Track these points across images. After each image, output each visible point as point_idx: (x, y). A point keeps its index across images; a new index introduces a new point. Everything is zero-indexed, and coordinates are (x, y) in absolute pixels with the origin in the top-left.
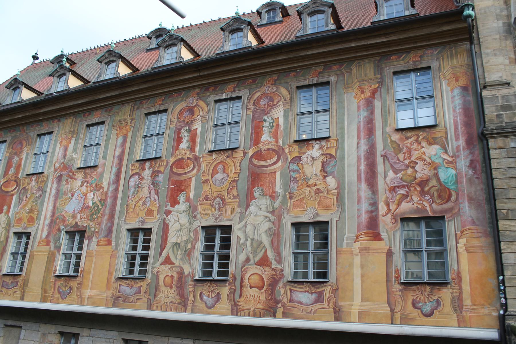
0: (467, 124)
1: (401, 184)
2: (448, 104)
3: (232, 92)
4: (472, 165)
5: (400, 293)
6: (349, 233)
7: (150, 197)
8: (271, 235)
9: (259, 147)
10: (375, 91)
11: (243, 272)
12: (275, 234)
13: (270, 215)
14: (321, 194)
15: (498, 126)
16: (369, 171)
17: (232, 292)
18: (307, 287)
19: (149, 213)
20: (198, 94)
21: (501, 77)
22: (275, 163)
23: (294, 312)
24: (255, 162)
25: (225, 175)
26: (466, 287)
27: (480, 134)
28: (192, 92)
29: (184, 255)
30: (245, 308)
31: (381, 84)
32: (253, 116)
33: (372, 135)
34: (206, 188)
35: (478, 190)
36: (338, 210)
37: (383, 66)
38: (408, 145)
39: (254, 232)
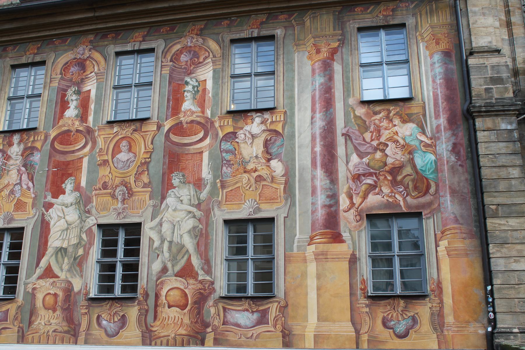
0: (449, 99)
1: (367, 171)
2: (426, 72)
3: (141, 42)
4: (455, 149)
6: (301, 234)
7: (20, 184)
8: (196, 236)
9: (179, 118)
10: (334, 52)
11: (159, 286)
12: (201, 235)
13: (194, 210)
14: (264, 183)
15: (487, 103)
16: (326, 153)
17: (143, 314)
18: (246, 304)
19: (20, 206)
20: (91, 42)
21: (490, 42)
22: (201, 140)
23: (229, 338)
24: (174, 138)
25: (131, 155)
26: (448, 300)
27: (465, 112)
28: (83, 39)
29: (73, 264)
30: (162, 334)
31: (342, 42)
32: (170, 76)
33: (331, 108)
34: (104, 172)
35: (462, 180)
36: (286, 203)
38: (377, 121)
39: (174, 233)
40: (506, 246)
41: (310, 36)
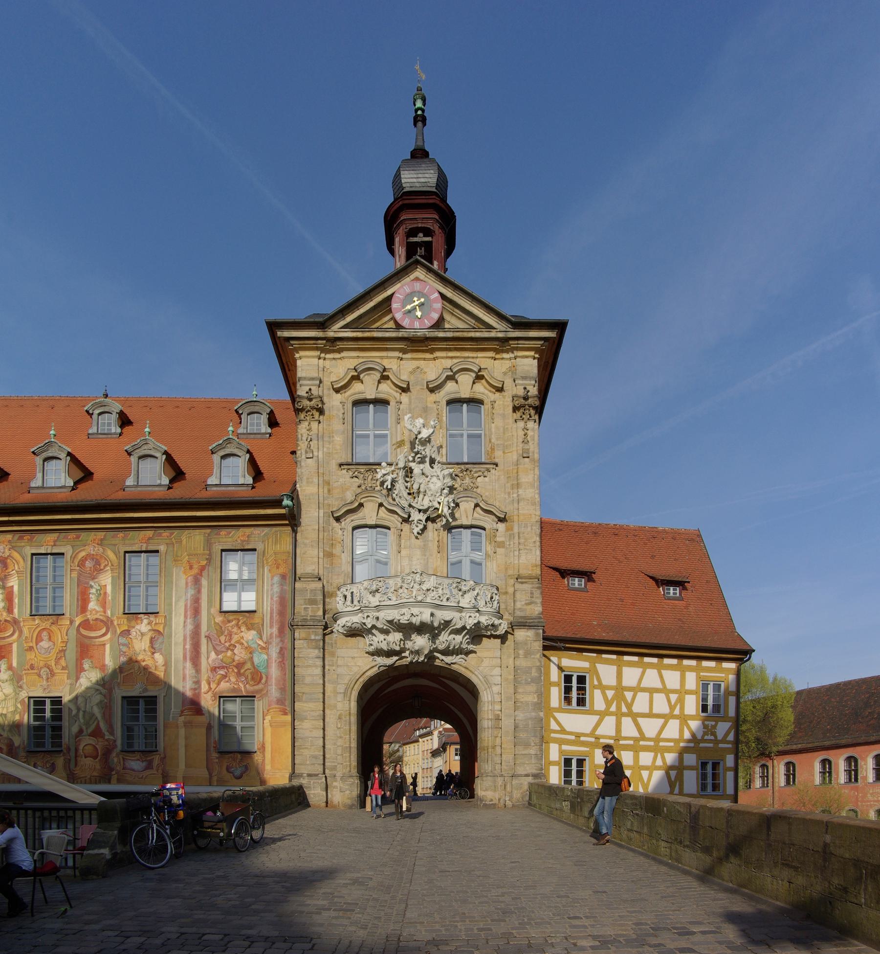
0: (282, 613)
2: (267, 591)
10: (202, 569)
18: (138, 755)
31: (209, 560)
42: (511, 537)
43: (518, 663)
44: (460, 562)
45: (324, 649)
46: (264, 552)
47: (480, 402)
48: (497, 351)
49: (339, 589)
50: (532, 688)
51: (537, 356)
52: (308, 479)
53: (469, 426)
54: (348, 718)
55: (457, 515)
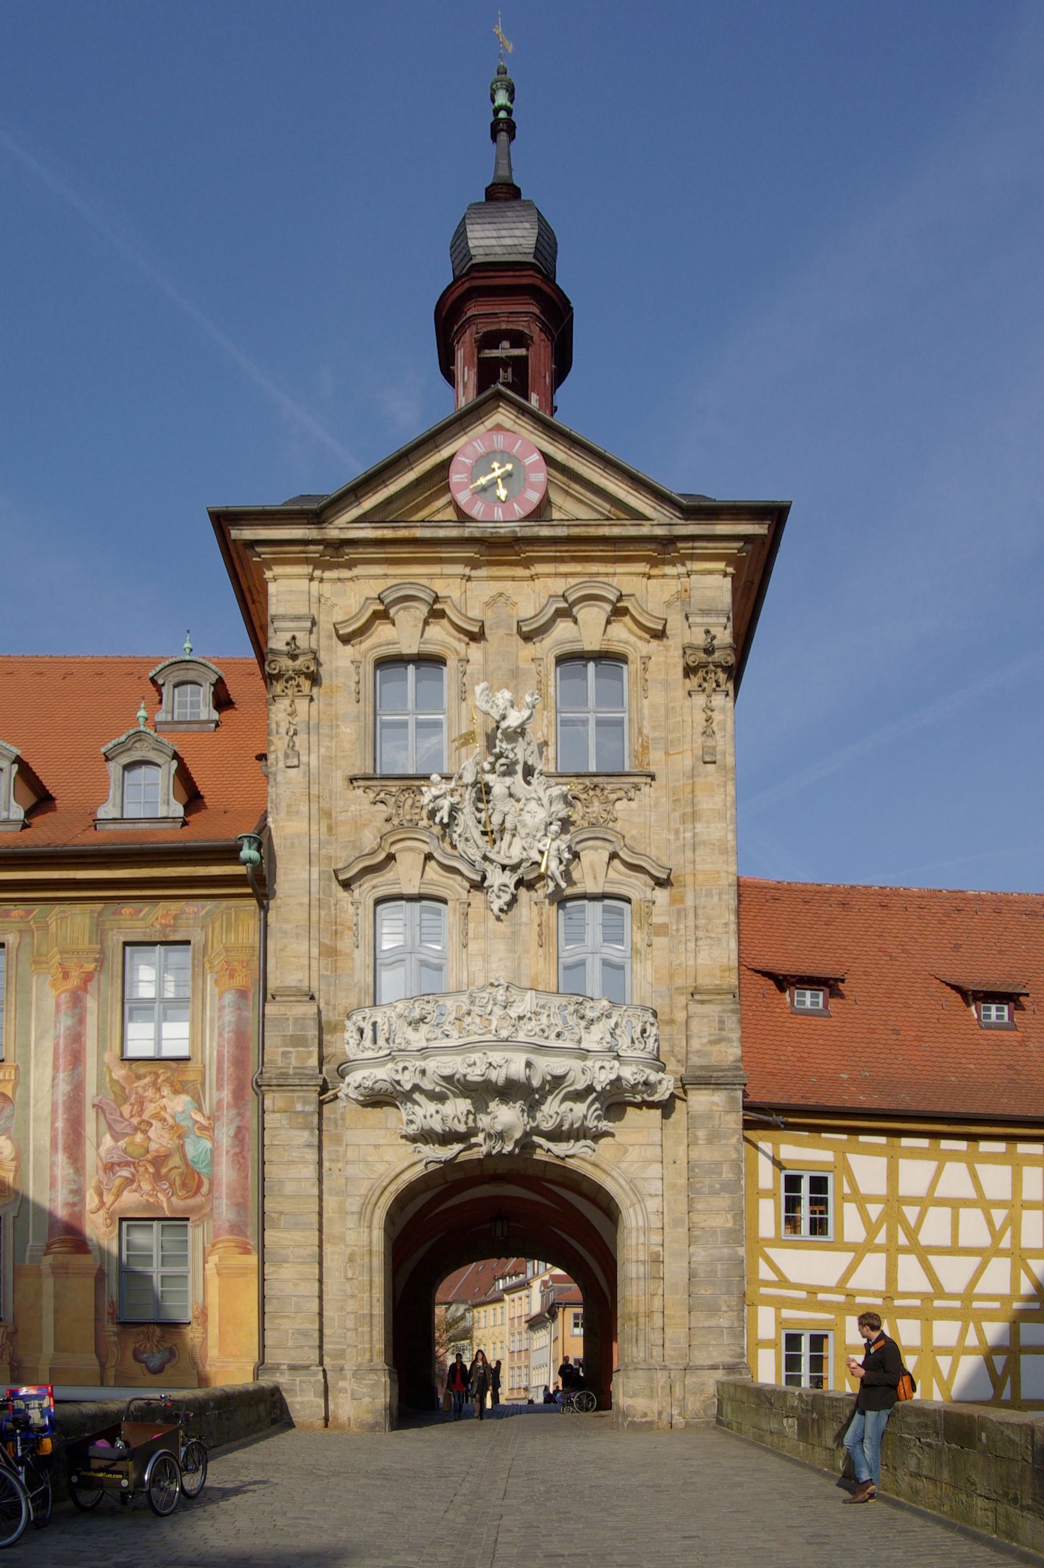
0: (239, 1063)
1: (123, 1160)
5: (115, 1339)
10: (88, 978)
21: (301, 981)
26: (213, 1329)
31: (101, 962)
37: (107, 925)
38: (140, 1090)
40: (285, 1265)
41: (56, 949)
42: (681, 914)
43: (694, 1154)
44: (582, 963)
45: (320, 1130)
46: (205, 947)
47: (621, 658)
48: (653, 562)
49: (349, 1017)
50: (723, 1201)
51: (730, 570)
52: (289, 806)
53: (599, 702)
54: (366, 1260)
55: (575, 875)
